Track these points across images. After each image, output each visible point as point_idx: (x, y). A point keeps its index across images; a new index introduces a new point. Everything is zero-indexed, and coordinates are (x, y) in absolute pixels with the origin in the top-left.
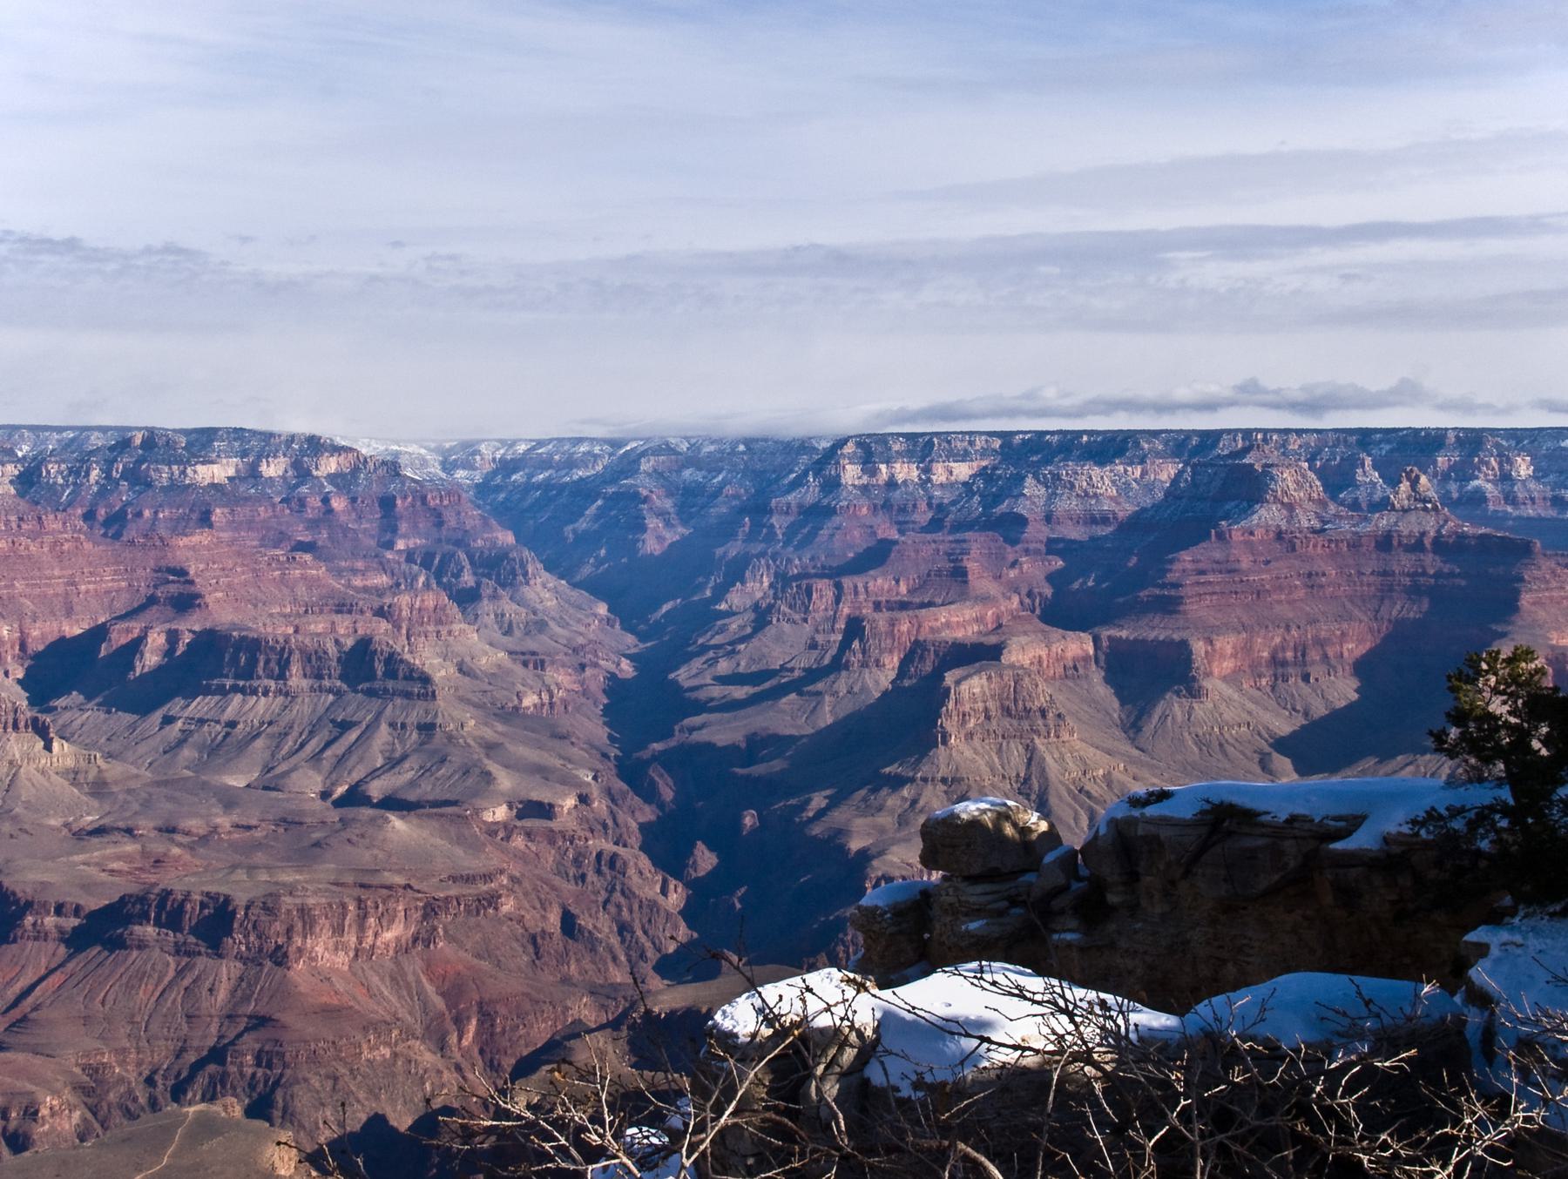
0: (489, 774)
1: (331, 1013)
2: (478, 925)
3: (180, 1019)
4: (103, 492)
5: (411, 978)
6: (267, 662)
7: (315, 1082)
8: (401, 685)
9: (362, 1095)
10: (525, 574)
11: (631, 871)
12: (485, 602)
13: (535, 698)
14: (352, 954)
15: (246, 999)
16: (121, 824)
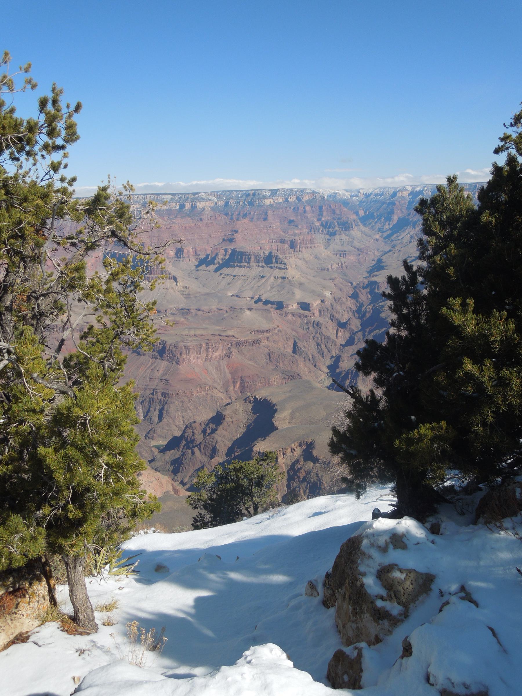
0: (294, 293)
1: (187, 381)
2: (253, 349)
3: (148, 379)
4: (243, 207)
5: (222, 368)
6: (245, 258)
7: (177, 403)
8: (279, 265)
9: (191, 408)
10: (352, 227)
11: (323, 327)
12: (337, 235)
13: (337, 265)
14: (204, 360)
15: (166, 374)
16: (187, 308)
